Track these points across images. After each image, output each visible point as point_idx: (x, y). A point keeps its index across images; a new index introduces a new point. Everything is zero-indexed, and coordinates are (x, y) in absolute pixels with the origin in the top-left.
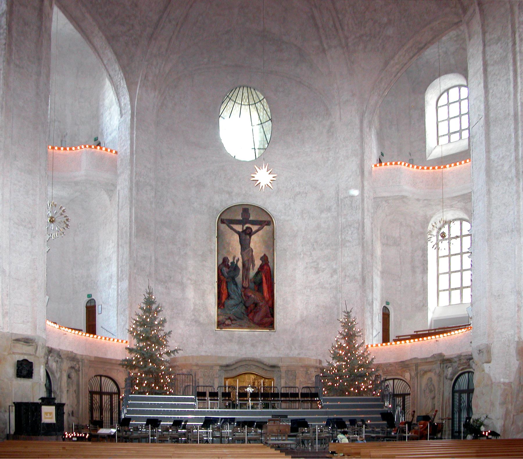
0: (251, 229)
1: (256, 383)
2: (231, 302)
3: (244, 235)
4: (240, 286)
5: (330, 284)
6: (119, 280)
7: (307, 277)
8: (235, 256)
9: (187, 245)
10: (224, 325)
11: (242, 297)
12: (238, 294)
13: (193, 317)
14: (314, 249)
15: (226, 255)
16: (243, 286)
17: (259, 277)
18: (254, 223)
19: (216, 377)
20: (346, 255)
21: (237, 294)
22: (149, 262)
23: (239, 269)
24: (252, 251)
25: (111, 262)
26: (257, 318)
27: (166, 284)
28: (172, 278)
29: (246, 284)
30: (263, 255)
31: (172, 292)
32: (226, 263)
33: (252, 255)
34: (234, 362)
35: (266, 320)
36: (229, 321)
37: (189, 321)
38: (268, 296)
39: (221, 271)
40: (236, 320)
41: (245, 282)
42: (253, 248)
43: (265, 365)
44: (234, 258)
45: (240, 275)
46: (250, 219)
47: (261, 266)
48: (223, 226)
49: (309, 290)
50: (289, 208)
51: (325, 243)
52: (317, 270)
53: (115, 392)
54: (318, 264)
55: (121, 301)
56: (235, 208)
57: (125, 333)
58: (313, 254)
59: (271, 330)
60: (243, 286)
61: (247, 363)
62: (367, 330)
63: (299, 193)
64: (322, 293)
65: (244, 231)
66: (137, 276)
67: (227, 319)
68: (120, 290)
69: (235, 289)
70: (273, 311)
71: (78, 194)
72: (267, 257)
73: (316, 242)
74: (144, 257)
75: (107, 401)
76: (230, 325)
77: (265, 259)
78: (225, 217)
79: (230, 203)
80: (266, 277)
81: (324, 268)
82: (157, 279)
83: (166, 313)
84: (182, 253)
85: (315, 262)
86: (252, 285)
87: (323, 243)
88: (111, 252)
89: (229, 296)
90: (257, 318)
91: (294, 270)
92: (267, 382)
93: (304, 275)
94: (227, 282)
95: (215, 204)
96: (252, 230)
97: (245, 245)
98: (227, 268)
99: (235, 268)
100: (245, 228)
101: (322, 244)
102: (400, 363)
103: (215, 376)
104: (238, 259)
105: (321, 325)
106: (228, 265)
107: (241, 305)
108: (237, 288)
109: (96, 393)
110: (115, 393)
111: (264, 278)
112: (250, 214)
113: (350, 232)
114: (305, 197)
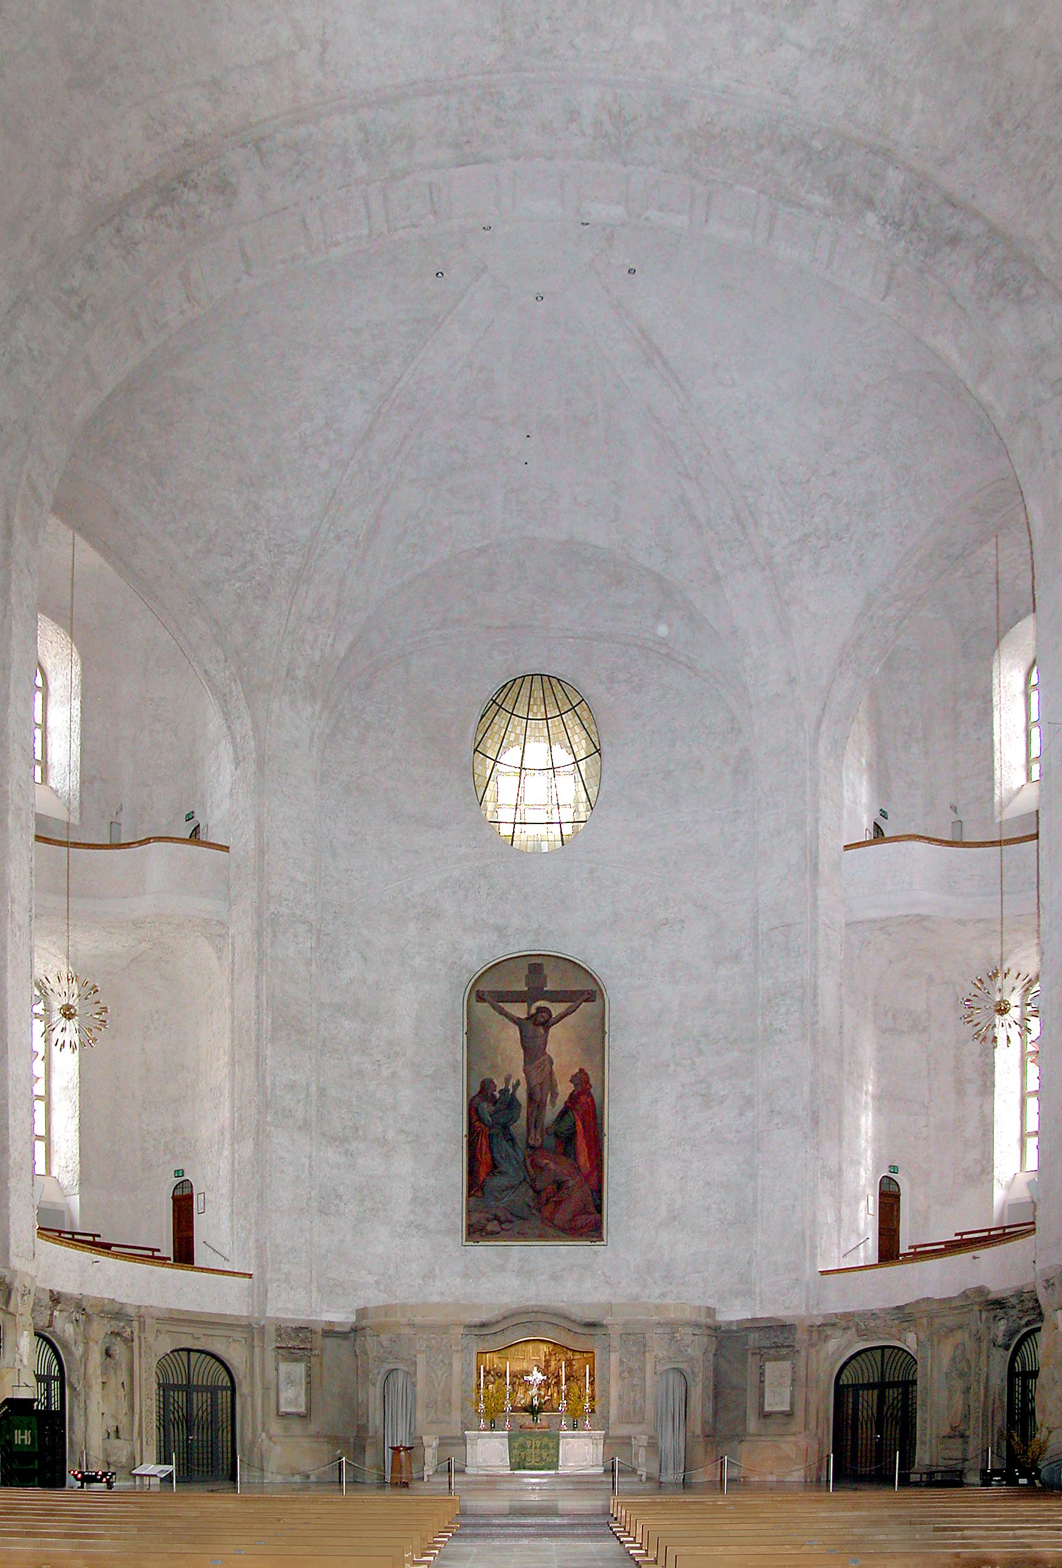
0: (549, 1010)
2: (499, 1181)
3: (531, 1026)
4: (521, 1144)
5: (737, 1131)
6: (236, 1139)
7: (685, 1118)
8: (511, 1075)
9: (396, 1053)
10: (484, 1233)
11: (526, 1168)
12: (518, 1162)
13: (412, 1217)
14: (700, 1052)
15: (488, 1075)
16: (528, 1143)
17: (568, 1120)
18: (556, 997)
19: (458, 1351)
20: (773, 1064)
21: (515, 1162)
22: (302, 1096)
23: (520, 1105)
24: (552, 1063)
25: (222, 1099)
26: (563, 1216)
27: (347, 1146)
28: (361, 1132)
29: (536, 1139)
30: (578, 1071)
31: (360, 1161)
32: (489, 1092)
33: (551, 1073)
34: (500, 1318)
35: (582, 1220)
36: (496, 1222)
37: (401, 1226)
38: (588, 1165)
39: (477, 1110)
40: (511, 1222)
41: (532, 1135)
42: (552, 1056)
43: (574, 1321)
44: (507, 1080)
45: (521, 1118)
46: (545, 989)
47: (571, 1094)
48: (484, 1009)
49: (688, 1148)
50: (641, 958)
51: (726, 1038)
52: (707, 1100)
53: (224, 1384)
54: (709, 1086)
55: (240, 1186)
56: (512, 963)
57: (247, 1257)
58: (697, 1064)
59: (595, 1242)
60: (528, 1143)
61: (532, 1317)
62: (825, 1237)
63: (666, 922)
64: (718, 1154)
65: (530, 1017)
66: (272, 1129)
67: (488, 1220)
68: (236, 1162)
69: (510, 1150)
70: (601, 1199)
71: (145, 946)
72: (586, 1074)
73: (706, 1035)
74: (292, 1087)
75: (205, 1405)
76: (499, 1233)
77: (581, 1080)
78: (488, 986)
79: (501, 953)
80: (583, 1120)
81: (724, 1096)
82: (323, 1135)
83: (347, 1210)
84: (385, 1072)
85: (701, 1081)
86: (550, 1142)
87: (720, 1037)
88: (223, 1075)
89: (494, 1167)
90: (561, 1217)
91: (655, 1101)
93: (677, 1112)
94: (490, 1137)
95: (466, 956)
96: (551, 1016)
97: (533, 1050)
98: (491, 1104)
99: (511, 1103)
100: (533, 1011)
101: (720, 1039)
102: (895, 1312)
103: (454, 1348)
104: (518, 1083)
105: (717, 1227)
106: (493, 1095)
107: (524, 1187)
108: (513, 1148)
109: (177, 1387)
110: (223, 1388)
111: (579, 1124)
112: (545, 978)
113: (783, 1010)
114: (680, 931)
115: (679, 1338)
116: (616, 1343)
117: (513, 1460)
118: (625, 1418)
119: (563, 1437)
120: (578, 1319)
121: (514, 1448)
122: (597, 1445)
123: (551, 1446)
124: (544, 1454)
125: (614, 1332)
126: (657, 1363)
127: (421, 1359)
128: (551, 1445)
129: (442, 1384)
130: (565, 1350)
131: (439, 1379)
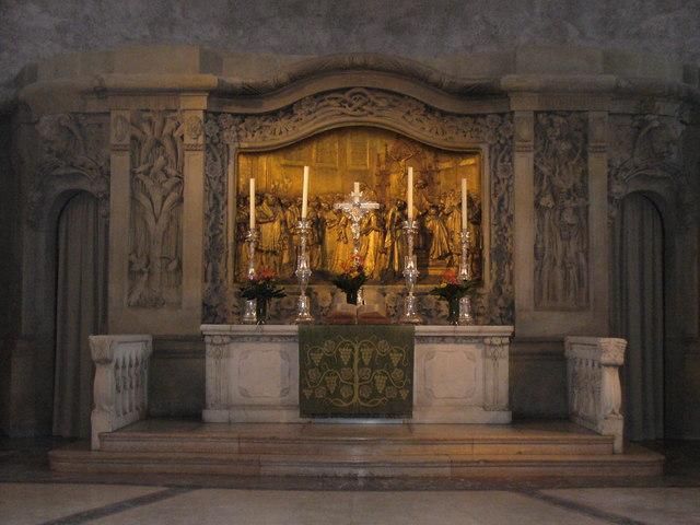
1: (394, 178)
19: (193, 148)
34: (283, 77)
43: (437, 86)
103: (188, 140)
115: (656, 124)
116: (525, 131)
117: (307, 393)
118: (544, 295)
119: (424, 339)
123: (395, 362)
124: (380, 382)
125: (522, 107)
127: (120, 164)
128: (395, 358)
129: (163, 220)
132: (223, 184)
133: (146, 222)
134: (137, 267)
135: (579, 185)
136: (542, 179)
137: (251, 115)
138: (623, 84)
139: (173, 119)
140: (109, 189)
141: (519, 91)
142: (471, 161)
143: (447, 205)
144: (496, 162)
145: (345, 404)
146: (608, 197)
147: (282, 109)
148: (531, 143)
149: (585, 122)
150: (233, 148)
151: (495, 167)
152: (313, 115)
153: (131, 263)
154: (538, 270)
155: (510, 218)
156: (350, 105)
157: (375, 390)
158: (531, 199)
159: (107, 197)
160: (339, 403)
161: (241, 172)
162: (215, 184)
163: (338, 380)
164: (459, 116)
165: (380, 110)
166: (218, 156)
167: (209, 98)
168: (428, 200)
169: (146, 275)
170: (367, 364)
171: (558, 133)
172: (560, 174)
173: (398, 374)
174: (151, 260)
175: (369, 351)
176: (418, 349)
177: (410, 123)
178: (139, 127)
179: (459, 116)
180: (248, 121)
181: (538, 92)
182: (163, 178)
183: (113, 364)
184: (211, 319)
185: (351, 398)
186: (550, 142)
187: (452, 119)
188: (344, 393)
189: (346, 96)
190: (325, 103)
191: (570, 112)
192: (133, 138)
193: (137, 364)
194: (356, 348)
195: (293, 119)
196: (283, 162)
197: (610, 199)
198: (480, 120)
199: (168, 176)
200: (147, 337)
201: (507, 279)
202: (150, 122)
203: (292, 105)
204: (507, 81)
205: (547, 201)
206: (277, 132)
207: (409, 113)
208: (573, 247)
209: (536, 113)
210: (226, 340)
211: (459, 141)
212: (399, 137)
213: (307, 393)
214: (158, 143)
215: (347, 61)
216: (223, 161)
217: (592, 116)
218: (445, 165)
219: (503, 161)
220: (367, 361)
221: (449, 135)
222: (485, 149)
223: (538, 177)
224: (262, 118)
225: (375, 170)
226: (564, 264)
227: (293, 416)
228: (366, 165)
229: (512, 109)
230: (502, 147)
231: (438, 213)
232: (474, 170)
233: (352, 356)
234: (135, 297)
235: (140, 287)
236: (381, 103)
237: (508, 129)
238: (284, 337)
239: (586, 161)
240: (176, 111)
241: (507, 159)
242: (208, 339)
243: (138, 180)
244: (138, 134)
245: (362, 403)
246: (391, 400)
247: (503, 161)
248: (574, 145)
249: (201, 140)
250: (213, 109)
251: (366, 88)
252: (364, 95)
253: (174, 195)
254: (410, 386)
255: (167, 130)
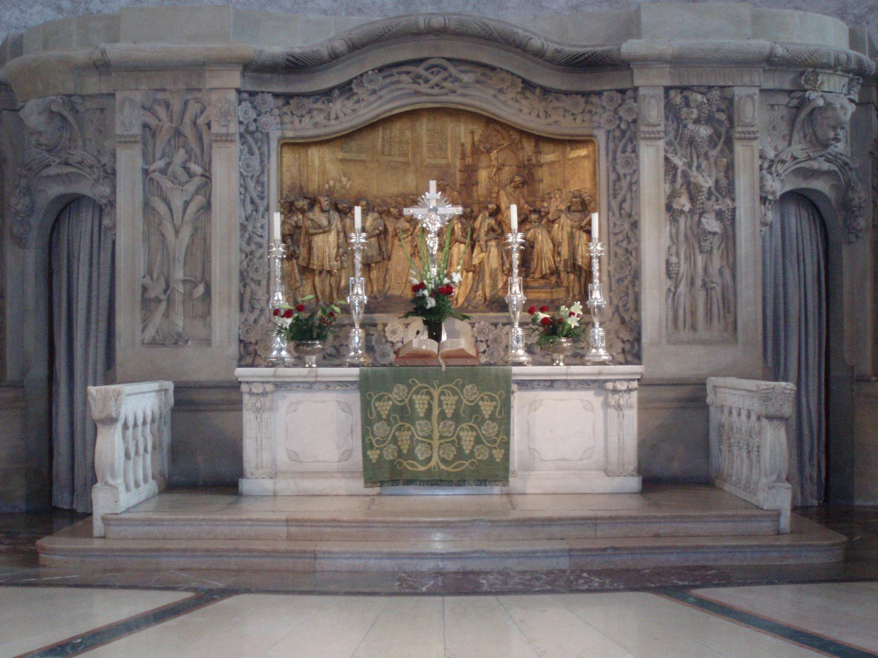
1: (483, 175)
34: (340, 46)
43: (539, 55)
92: (552, 163)
103: (216, 128)
115: (821, 102)
117: (373, 455)
120: (551, 47)
121: (380, 418)
122: (619, 407)
124: (467, 439)
126: (764, 172)
128: (487, 408)
129: (186, 233)
130: (516, 136)
131: (178, 214)
132: (263, 185)
133: (163, 236)
134: (152, 294)
135: (724, 182)
136: (675, 175)
137: (298, 95)
138: (780, 51)
139: (197, 101)
140: (114, 192)
141: (646, 62)
142: (583, 152)
143: (552, 209)
144: (615, 152)
145: (422, 468)
146: (761, 198)
147: (339, 87)
148: (662, 128)
149: (731, 101)
150: (275, 135)
151: (614, 159)
152: (379, 93)
153: (145, 289)
154: (672, 293)
155: (635, 225)
156: (427, 81)
157: (460, 450)
158: (663, 201)
159: (112, 204)
160: (413, 466)
161: (285, 169)
162: (251, 185)
163: (412, 436)
164: (567, 93)
165: (466, 86)
166: (255, 149)
167: (243, 74)
168: (527, 202)
169: (163, 306)
170: (449, 416)
171: (694, 116)
172: (699, 167)
173: (490, 429)
174: (172, 285)
175: (452, 399)
176: (519, 399)
177: (505, 103)
178: (154, 114)
179: (567, 93)
180: (293, 102)
181: (670, 62)
182: (184, 177)
183: (119, 426)
184: (249, 360)
185: (429, 459)
186: (685, 126)
187: (558, 99)
188: (420, 452)
189: (420, 70)
190: (394, 79)
191: (710, 88)
192: (146, 126)
193: (153, 421)
194: (436, 394)
195: (356, 98)
196: (340, 155)
197: (764, 200)
198: (594, 99)
199: (191, 175)
200: (170, 385)
201: (631, 305)
202: (168, 105)
203: (350, 82)
204: (630, 47)
205: (683, 202)
206: (333, 116)
207: (501, 91)
208: (717, 262)
209: (667, 89)
210: (269, 388)
211: (567, 126)
212: (490, 121)
213: (373, 455)
214: (178, 133)
215: (422, 24)
216: (261, 154)
217: (739, 92)
218: (549, 156)
219: (624, 151)
220: (449, 412)
221: (552, 120)
222: (601, 137)
223: (670, 168)
224: (311, 99)
225: (458, 163)
226: (704, 284)
227: (358, 485)
228: (446, 158)
229: (637, 82)
230: (623, 133)
231: (541, 218)
232: (587, 165)
233: (430, 405)
234: (151, 332)
235: (158, 318)
236: (467, 78)
237: (630, 110)
238: (344, 384)
239: (731, 151)
240: (199, 90)
241: (629, 148)
242: (244, 388)
243: (152, 180)
244: (152, 121)
245: (443, 467)
246: (481, 461)
247: (624, 151)
248: (715, 131)
249: (234, 128)
250: (249, 88)
251: (449, 60)
252: (445, 69)
253: (199, 199)
254: (506, 445)
255: (187, 120)
